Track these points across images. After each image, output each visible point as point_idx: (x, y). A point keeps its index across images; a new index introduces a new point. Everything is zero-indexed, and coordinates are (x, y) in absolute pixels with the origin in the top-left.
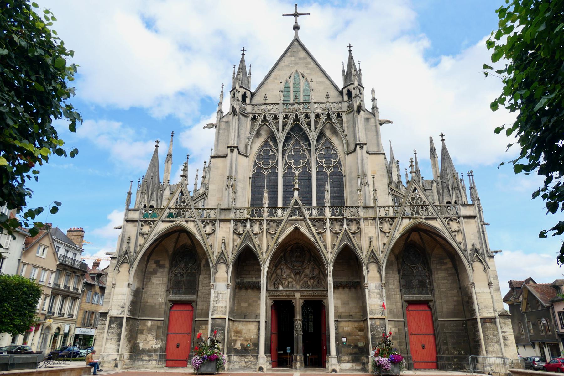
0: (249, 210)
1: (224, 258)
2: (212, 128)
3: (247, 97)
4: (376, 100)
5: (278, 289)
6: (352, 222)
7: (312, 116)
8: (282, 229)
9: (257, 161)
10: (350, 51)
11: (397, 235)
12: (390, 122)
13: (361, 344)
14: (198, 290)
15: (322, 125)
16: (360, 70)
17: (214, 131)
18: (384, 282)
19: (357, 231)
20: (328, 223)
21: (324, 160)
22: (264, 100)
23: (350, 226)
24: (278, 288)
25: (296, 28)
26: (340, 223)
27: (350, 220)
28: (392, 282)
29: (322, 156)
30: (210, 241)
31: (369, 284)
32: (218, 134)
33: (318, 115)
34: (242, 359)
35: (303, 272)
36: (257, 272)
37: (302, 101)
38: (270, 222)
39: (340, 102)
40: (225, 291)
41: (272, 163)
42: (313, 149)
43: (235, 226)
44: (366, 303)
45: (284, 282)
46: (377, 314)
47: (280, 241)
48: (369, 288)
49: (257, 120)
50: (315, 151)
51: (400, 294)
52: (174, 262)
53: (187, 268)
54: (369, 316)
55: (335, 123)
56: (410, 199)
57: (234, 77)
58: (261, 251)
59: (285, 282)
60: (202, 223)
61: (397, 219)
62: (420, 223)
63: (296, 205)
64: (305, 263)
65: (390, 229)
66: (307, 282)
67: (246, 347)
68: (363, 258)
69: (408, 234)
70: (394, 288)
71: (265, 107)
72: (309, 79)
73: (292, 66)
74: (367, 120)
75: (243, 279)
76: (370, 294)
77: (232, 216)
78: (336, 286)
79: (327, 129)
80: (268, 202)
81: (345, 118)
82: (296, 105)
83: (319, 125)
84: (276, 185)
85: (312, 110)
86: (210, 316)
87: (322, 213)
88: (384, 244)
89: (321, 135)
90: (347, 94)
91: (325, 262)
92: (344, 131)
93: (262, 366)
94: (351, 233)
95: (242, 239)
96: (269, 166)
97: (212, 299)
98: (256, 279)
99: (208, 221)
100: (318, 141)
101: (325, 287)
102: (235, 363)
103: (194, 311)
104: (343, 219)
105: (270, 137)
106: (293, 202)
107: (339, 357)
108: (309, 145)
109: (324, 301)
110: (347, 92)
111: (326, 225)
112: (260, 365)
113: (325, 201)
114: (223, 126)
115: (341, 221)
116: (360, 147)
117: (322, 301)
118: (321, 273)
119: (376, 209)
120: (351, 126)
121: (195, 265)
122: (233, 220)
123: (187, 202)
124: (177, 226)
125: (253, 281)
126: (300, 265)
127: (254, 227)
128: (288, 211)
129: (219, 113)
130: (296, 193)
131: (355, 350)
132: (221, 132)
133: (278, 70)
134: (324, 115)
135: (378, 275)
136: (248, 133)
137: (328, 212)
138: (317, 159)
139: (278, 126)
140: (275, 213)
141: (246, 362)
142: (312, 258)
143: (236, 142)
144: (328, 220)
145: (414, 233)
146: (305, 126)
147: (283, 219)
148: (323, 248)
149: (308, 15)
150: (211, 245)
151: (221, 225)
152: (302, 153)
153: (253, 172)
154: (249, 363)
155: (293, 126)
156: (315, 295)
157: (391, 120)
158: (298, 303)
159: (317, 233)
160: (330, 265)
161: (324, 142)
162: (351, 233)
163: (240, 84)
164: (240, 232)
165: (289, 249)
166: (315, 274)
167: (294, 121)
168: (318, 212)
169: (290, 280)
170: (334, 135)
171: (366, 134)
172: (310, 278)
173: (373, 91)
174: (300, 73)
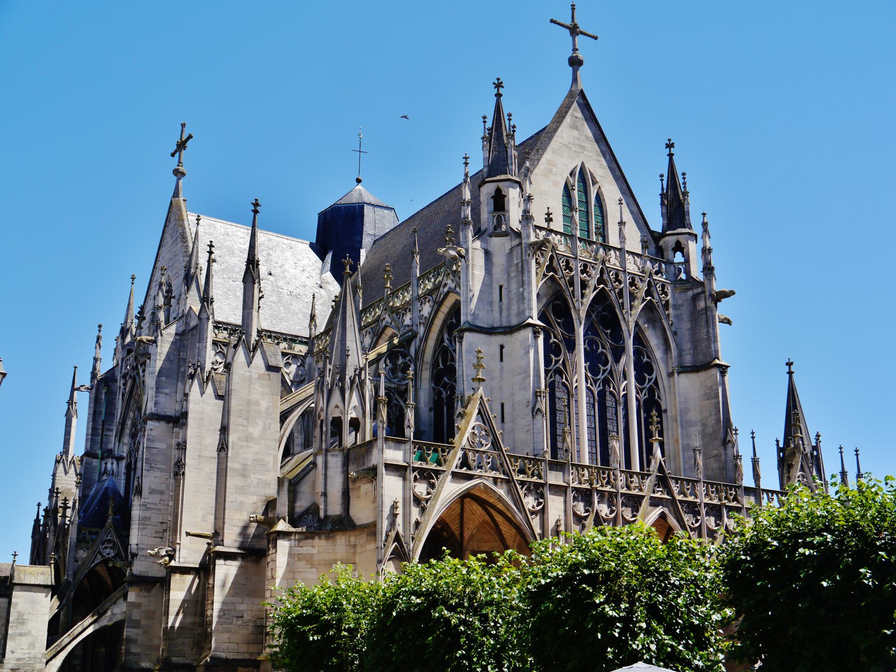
20: (704, 511)
25: (575, 63)
60: (522, 488)
73: (575, 151)
133: (554, 152)
144: (703, 505)
147: (644, 497)
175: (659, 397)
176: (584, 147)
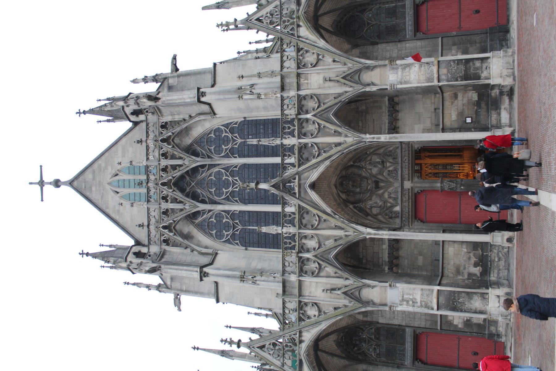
0: (285, 254)
1: (353, 290)
2: (180, 299)
3: (140, 251)
4: (146, 77)
5: (399, 213)
6: (303, 106)
7: (165, 162)
8: (313, 207)
9: (224, 240)
10: (84, 112)
11: (322, 43)
12: (174, 58)
13: (474, 96)
14: (399, 325)
15: (175, 149)
16: (108, 99)
17: (184, 298)
18: (387, 62)
19: (316, 100)
21: (223, 146)
22: (143, 228)
23: (309, 109)
24: (397, 213)
25: (57, 183)
26: (305, 122)
27: (301, 109)
28: (389, 53)
29: (217, 149)
30: (330, 310)
31: (391, 82)
32: (188, 292)
33: (163, 155)
34: (495, 265)
35: (375, 177)
36: (375, 242)
37: (145, 177)
38: (302, 224)
39: (147, 125)
40: (400, 290)
41: (227, 218)
42: (208, 162)
43: (308, 273)
44: (417, 87)
45: (389, 205)
46: (432, 71)
47: (329, 210)
48: (396, 83)
49: (169, 238)
50: (210, 159)
51: (405, 42)
52: (360, 357)
53: (369, 340)
54: (436, 83)
55: (173, 132)
56: (271, 26)
57: (115, 268)
58: (344, 237)
59: (390, 203)
60: (304, 320)
61: (299, 44)
62: (305, 13)
63: (279, 186)
64: (364, 174)
65: (314, 53)
66: (389, 171)
67: (479, 259)
68: (354, 92)
69: (322, 31)
70: (397, 50)
71: (152, 228)
72: (119, 167)
73: (103, 190)
74: (170, 88)
75: (385, 261)
76: (405, 82)
77: (293, 278)
78: (394, 129)
79: (182, 141)
80: (274, 226)
81: (167, 118)
82: (150, 184)
83: (175, 153)
84: (256, 214)
85: (156, 163)
86: (435, 312)
87: (291, 149)
88: (334, 61)
89: (191, 151)
90: (137, 116)
91: (359, 145)
92: (184, 120)
93: (506, 238)
94: (318, 107)
95: (327, 265)
96: (231, 222)
97: (411, 309)
98: (385, 244)
99: (301, 312)
100: (197, 155)
101: (397, 146)
102: (501, 275)
103: (428, 331)
104: (299, 120)
105: (192, 221)
106: (274, 191)
107: (492, 128)
108: (203, 166)
109: (416, 149)
110: (135, 116)
111: (307, 144)
112: (505, 241)
113: (273, 145)
114: (176, 285)
115: (302, 123)
116: (203, 96)
117: (416, 150)
118: (378, 152)
119: (285, 72)
120: (177, 109)
121: (364, 329)
122: (300, 276)
123: (274, 341)
124: (307, 355)
125: (387, 248)
126: (366, 180)
127: (309, 247)
128: (288, 198)
129: (160, 289)
130: (263, 186)
131: (483, 105)
132: (184, 288)
134: (163, 147)
135: (377, 71)
136: (185, 251)
137: (290, 141)
138: (221, 157)
139: (177, 209)
140: (290, 216)
141: (499, 259)
142: (356, 164)
143: (196, 269)
144: (300, 141)
145: (320, 22)
146: (177, 174)
147: (299, 205)
148: (339, 148)
149: (42, 168)
150: (335, 309)
151: (307, 294)
152: (213, 178)
153: (239, 245)
154: (501, 255)
155: (178, 189)
156: (407, 161)
157: (172, 56)
158: (418, 185)
159: (318, 156)
160: (363, 138)
161: (200, 146)
162: (318, 107)
163: (123, 260)
164: (316, 268)
165: (344, 196)
166: (378, 160)
167: (171, 189)
168: (290, 156)
169: (386, 195)
170: (190, 133)
171: (189, 89)
172: (384, 167)
173: (135, 81)
174: (112, 179)
175: (236, 124)
176: (100, 182)
